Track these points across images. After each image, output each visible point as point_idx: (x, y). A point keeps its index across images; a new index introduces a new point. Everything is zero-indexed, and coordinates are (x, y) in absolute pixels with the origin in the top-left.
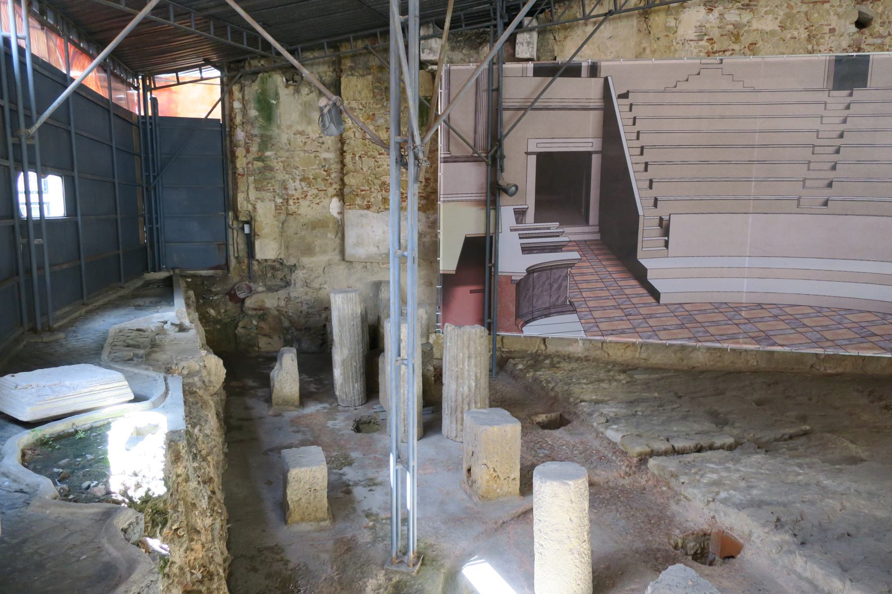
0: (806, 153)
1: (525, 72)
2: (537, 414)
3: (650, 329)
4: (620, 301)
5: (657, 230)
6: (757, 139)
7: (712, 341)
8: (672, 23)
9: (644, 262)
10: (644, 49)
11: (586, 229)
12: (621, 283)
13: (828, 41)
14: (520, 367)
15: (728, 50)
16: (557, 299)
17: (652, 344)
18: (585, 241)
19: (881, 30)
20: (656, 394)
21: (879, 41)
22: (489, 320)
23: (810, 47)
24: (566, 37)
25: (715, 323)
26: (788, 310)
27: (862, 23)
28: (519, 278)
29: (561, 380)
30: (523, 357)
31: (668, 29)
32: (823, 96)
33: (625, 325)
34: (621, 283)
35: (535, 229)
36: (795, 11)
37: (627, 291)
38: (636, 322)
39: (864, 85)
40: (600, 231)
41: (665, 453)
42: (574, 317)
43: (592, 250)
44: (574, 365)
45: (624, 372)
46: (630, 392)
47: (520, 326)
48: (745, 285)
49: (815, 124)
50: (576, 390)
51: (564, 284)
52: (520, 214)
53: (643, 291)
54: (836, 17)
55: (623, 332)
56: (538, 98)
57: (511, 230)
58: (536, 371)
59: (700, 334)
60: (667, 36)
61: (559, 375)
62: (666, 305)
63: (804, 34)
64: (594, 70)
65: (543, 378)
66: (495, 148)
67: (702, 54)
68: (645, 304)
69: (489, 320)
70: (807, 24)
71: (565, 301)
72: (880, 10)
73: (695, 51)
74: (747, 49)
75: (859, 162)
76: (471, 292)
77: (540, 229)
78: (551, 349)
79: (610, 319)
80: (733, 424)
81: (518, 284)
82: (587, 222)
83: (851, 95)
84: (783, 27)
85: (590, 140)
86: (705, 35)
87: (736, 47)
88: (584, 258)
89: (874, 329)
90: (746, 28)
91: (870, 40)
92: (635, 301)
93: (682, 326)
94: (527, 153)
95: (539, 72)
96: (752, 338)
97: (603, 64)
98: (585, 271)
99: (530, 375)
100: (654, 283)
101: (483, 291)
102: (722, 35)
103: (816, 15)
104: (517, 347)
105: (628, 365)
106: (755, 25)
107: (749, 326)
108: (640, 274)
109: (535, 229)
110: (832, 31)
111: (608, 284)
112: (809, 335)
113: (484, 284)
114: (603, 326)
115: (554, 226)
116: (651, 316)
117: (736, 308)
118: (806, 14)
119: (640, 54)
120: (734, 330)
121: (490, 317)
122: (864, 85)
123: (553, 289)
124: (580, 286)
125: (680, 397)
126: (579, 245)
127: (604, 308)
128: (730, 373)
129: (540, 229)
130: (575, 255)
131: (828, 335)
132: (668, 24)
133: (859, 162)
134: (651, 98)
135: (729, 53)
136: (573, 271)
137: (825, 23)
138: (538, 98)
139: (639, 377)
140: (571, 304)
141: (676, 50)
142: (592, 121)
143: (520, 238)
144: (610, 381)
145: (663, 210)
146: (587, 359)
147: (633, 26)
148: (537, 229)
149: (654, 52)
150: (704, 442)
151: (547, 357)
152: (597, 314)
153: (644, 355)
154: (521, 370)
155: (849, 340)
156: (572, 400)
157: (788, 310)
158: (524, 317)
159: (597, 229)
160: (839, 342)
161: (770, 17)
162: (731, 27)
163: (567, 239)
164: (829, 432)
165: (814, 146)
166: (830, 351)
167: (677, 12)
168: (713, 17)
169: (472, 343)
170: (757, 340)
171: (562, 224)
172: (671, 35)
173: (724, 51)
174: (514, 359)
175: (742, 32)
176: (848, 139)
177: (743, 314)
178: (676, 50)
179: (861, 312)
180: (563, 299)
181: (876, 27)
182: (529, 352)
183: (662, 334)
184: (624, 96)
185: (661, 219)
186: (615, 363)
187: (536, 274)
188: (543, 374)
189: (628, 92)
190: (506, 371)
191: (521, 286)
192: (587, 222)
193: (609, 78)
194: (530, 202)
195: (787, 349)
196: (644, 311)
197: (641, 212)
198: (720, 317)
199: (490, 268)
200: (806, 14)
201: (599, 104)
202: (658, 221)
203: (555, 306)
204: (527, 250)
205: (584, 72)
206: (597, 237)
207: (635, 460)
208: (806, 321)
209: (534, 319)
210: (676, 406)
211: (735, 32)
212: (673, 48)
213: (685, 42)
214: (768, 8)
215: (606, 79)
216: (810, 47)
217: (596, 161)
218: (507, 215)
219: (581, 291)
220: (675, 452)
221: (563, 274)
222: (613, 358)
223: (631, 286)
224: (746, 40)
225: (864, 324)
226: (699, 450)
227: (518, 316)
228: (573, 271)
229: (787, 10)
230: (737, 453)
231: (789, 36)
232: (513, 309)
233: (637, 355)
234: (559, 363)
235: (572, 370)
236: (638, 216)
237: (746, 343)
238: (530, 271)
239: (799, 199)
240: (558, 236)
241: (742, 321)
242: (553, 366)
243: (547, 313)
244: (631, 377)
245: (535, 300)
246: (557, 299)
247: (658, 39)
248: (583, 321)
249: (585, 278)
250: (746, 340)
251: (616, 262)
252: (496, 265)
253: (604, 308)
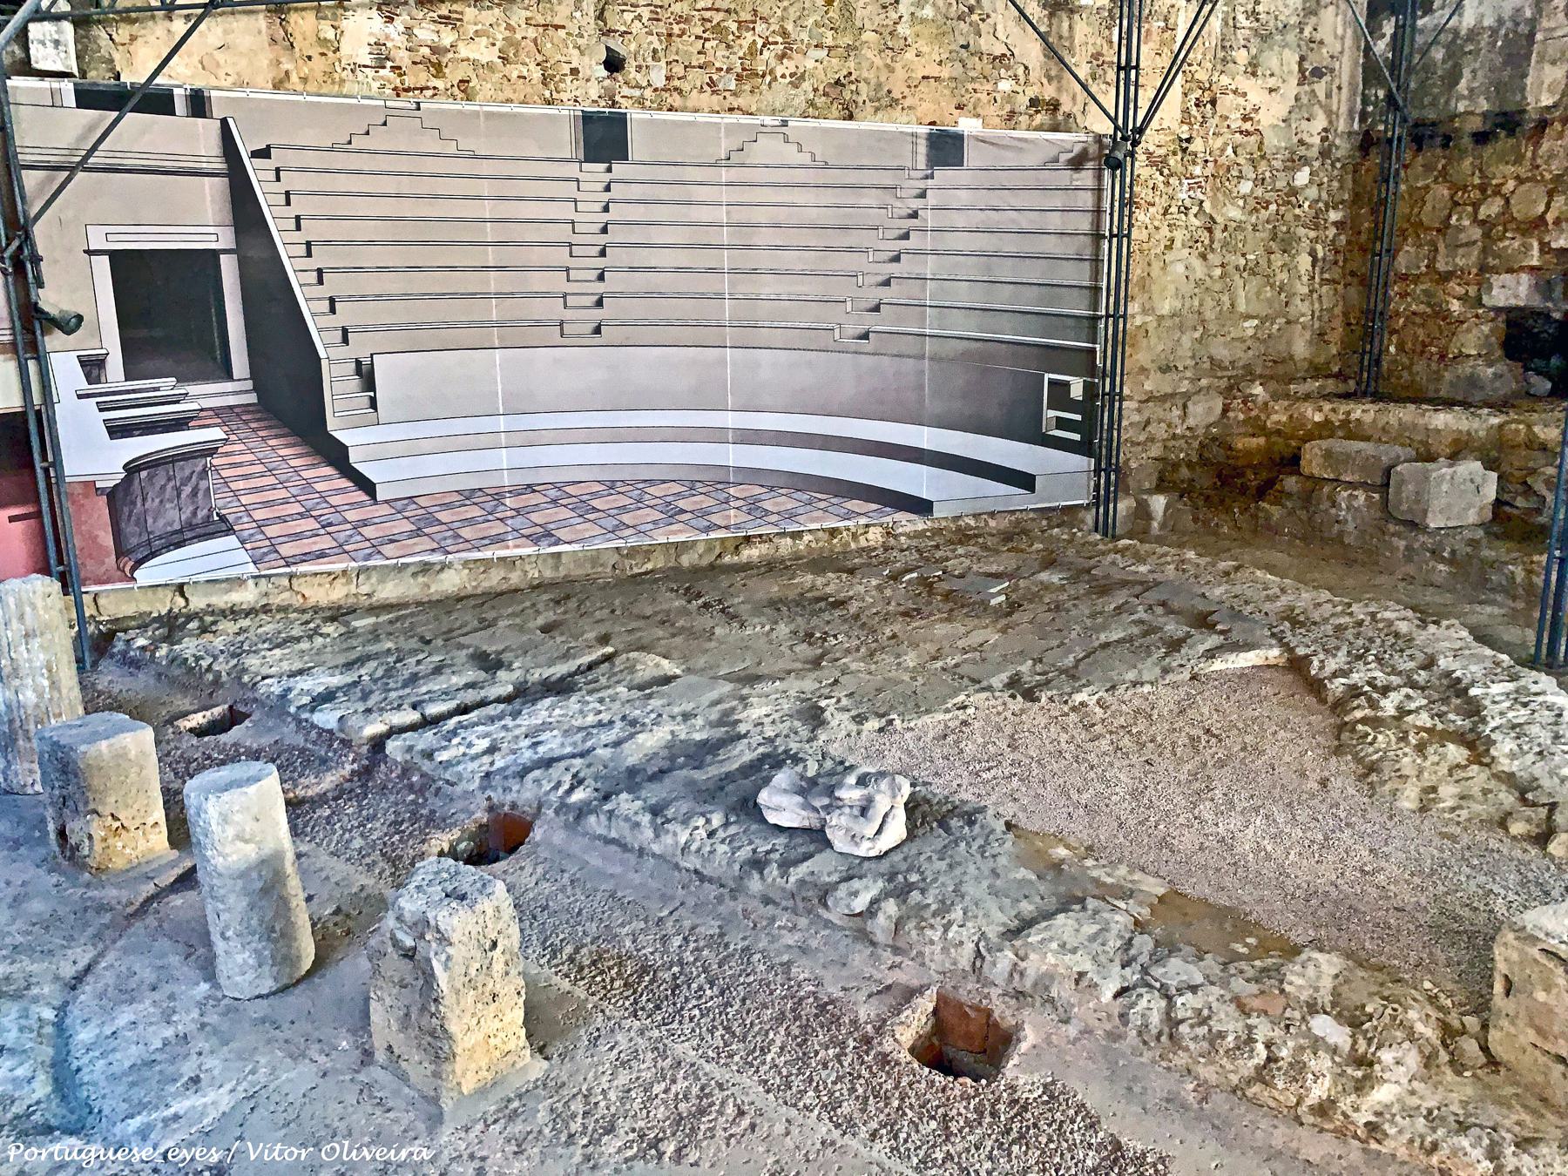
0: (561, 256)
1: (57, 97)
2: (185, 715)
3: (368, 544)
4: (309, 504)
5: (355, 382)
6: (490, 232)
7: (469, 550)
8: (330, 34)
9: (340, 436)
10: (287, 73)
11: (229, 386)
12: (305, 474)
13: (570, 88)
14: (141, 642)
15: (427, 88)
16: (194, 513)
17: (375, 567)
18: (231, 407)
19: (638, 76)
20: (390, 645)
21: (637, 93)
22: (61, 568)
23: (547, 94)
24: (133, 38)
25: (470, 522)
26: (569, 489)
27: (614, 64)
28: (111, 484)
29: (222, 652)
30: (143, 627)
31: (323, 42)
32: (572, 170)
33: (324, 543)
34: (305, 474)
35: (128, 392)
36: (518, 36)
37: (319, 487)
38: (342, 537)
39: (624, 157)
40: (255, 389)
41: (413, 727)
42: (232, 541)
43: (246, 422)
44: (245, 623)
45: (333, 619)
46: (348, 649)
47: (127, 569)
48: (503, 458)
49: (566, 211)
50: (252, 662)
51: (203, 484)
52: (93, 367)
53: (345, 483)
54: (576, 52)
55: (322, 555)
56: (94, 148)
57: (80, 397)
58: (173, 644)
59: (449, 542)
60: (323, 54)
61: (219, 642)
62: (386, 502)
63: (537, 74)
64: (199, 104)
65: (188, 654)
66: (16, 244)
67: (388, 92)
68: (354, 505)
69: (61, 568)
70: (540, 58)
71: (209, 516)
72: (633, 47)
73: (375, 85)
74: (455, 89)
75: (633, 269)
76: (12, 519)
77: (140, 391)
78: (198, 602)
79: (298, 536)
80: (511, 664)
81: (112, 495)
82: (229, 376)
83: (609, 170)
84: (505, 60)
85: (211, 230)
86: (388, 59)
87: (439, 84)
88: (233, 437)
89: (681, 504)
90: (450, 55)
91: (626, 91)
92: (334, 500)
93: (418, 532)
94: (89, 252)
95: (87, 98)
96: (527, 537)
97: (214, 94)
98: (238, 459)
99: (163, 651)
100: (359, 467)
101: (38, 515)
102: (414, 63)
103: (549, 45)
104: (128, 610)
105: (340, 607)
106: (464, 51)
107: (520, 519)
108: (337, 456)
109: (128, 392)
110: (574, 71)
111: (283, 477)
112: (601, 522)
113: (38, 501)
114: (286, 550)
115: (166, 385)
116: (365, 523)
117: (498, 497)
118: (535, 41)
119: (281, 82)
120: (498, 528)
121: (60, 562)
122: (624, 157)
123: (183, 496)
124: (233, 486)
125: (428, 642)
126: (223, 415)
127: (282, 520)
128: (502, 594)
129: (140, 391)
130: (216, 433)
131: (626, 518)
132: (322, 35)
133: (633, 269)
134: (311, 159)
135: (430, 92)
136: (215, 462)
137: (563, 59)
138: (94, 148)
139: (362, 623)
140: (223, 518)
141: (342, 81)
142: (211, 195)
143: (101, 410)
144: (310, 637)
145: (360, 347)
146: (266, 609)
147: (260, 32)
148: (134, 391)
149: (304, 80)
150: (470, 696)
151: (190, 617)
152: (271, 531)
153: (365, 589)
154: (143, 648)
155: (654, 522)
156: (246, 679)
157: (569, 489)
159: (249, 385)
160: (642, 528)
161: (484, 41)
162: (426, 51)
163: (195, 406)
164: (637, 650)
165: (571, 245)
166: (633, 542)
167: (335, 16)
168: (395, 32)
169: (28, 610)
170: (535, 540)
171: (182, 379)
172: (330, 54)
173: (422, 89)
174: (125, 631)
175: (444, 61)
176: (615, 235)
177: (507, 502)
178: (342, 81)
179: (664, 482)
180: (205, 511)
181: (630, 66)
182: (155, 615)
183: (388, 550)
184: (264, 153)
185: (358, 363)
186: (316, 609)
187: (144, 474)
188: (189, 647)
189: (269, 147)
190: (112, 656)
191: (118, 497)
192: (229, 376)
193: (230, 121)
195: (576, 547)
196: (352, 516)
197: (322, 354)
198: (475, 512)
199: (46, 471)
200: (535, 41)
201: (219, 165)
202: (353, 365)
203: (190, 526)
204: (118, 431)
205: (180, 105)
206: (252, 398)
207: (365, 749)
208: (595, 503)
209: (153, 555)
210: (421, 657)
211: (434, 59)
212: (336, 76)
213: (355, 68)
214: (479, 27)
215: (224, 122)
216: (547, 94)
217: (228, 266)
219: (236, 494)
220: (428, 722)
221: (199, 468)
222: (311, 602)
223: (325, 477)
224: (454, 74)
225: (668, 499)
226: (464, 710)
227: (120, 552)
228: (215, 462)
229: (507, 33)
230: (517, 703)
231: (515, 75)
232: (108, 540)
233: (353, 590)
234: (214, 623)
235: (242, 631)
236: (319, 359)
237: (517, 546)
238: (132, 469)
239: (561, 325)
240: (177, 402)
241: (509, 514)
242: (204, 630)
243: (177, 540)
244: (347, 624)
245: (150, 521)
246: (194, 513)
247: (310, 58)
248: (248, 546)
249: (240, 471)
250: (519, 541)
251: (290, 440)
252: (57, 463)
253: (282, 520)
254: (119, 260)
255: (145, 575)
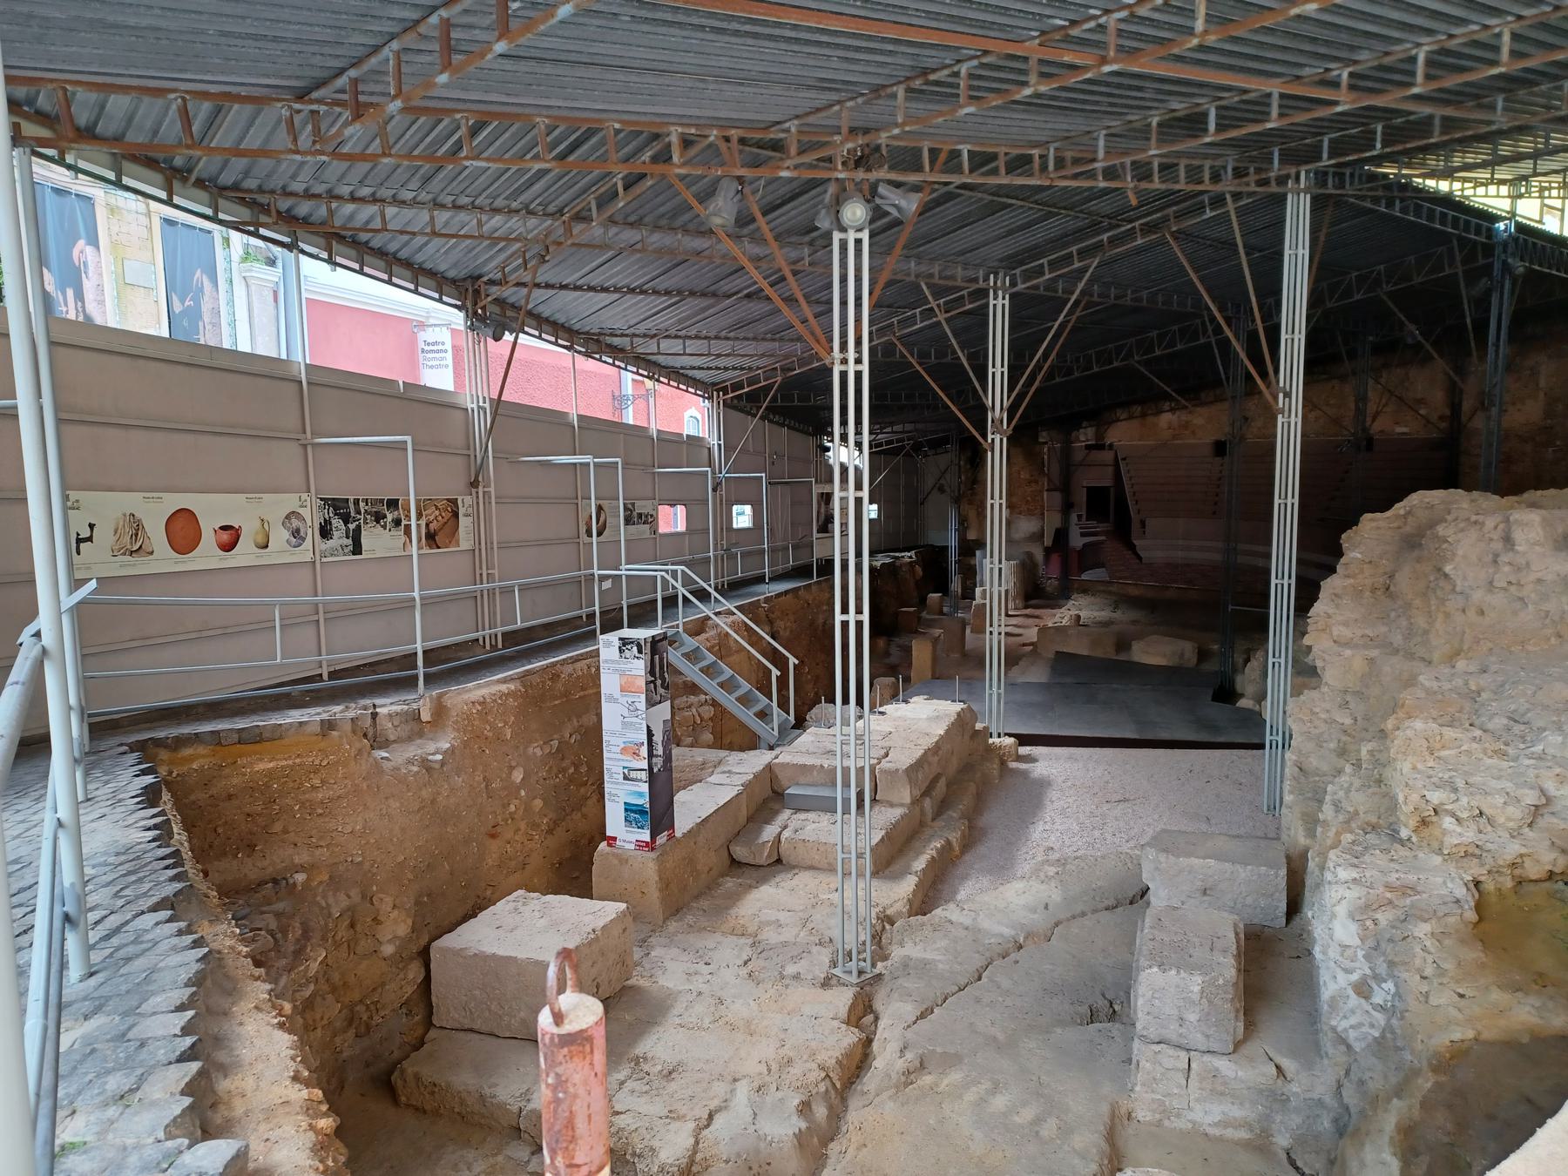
48: (1180, 554)
52: (1079, 517)
106: (1195, 422)
108: (1132, 548)
130: (1103, 538)
142: (1110, 470)
158: (1082, 570)
171: (1099, 522)
184: (1124, 459)
194: (1084, 513)
204: (1083, 535)
217: (1112, 490)
218: (1074, 518)
254: (1089, 489)
255: (1084, 577)
